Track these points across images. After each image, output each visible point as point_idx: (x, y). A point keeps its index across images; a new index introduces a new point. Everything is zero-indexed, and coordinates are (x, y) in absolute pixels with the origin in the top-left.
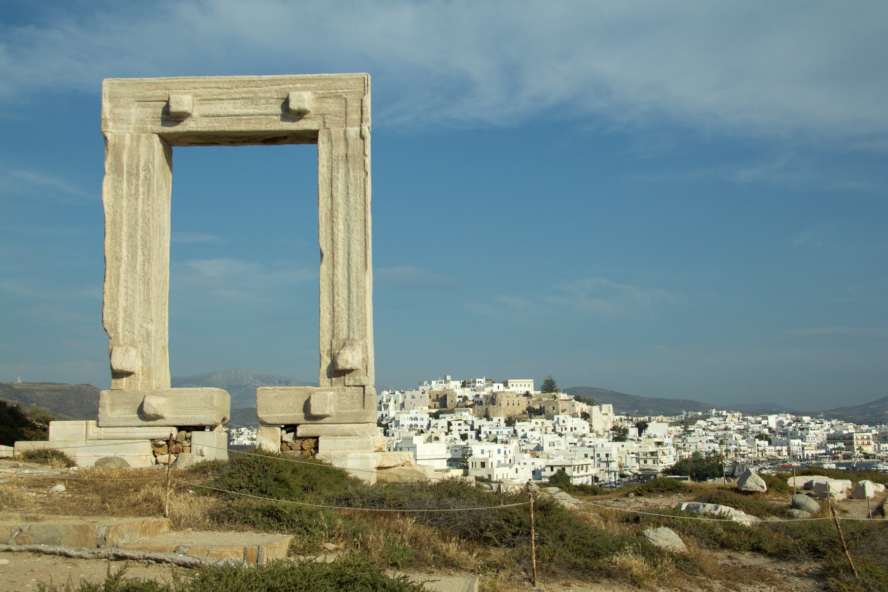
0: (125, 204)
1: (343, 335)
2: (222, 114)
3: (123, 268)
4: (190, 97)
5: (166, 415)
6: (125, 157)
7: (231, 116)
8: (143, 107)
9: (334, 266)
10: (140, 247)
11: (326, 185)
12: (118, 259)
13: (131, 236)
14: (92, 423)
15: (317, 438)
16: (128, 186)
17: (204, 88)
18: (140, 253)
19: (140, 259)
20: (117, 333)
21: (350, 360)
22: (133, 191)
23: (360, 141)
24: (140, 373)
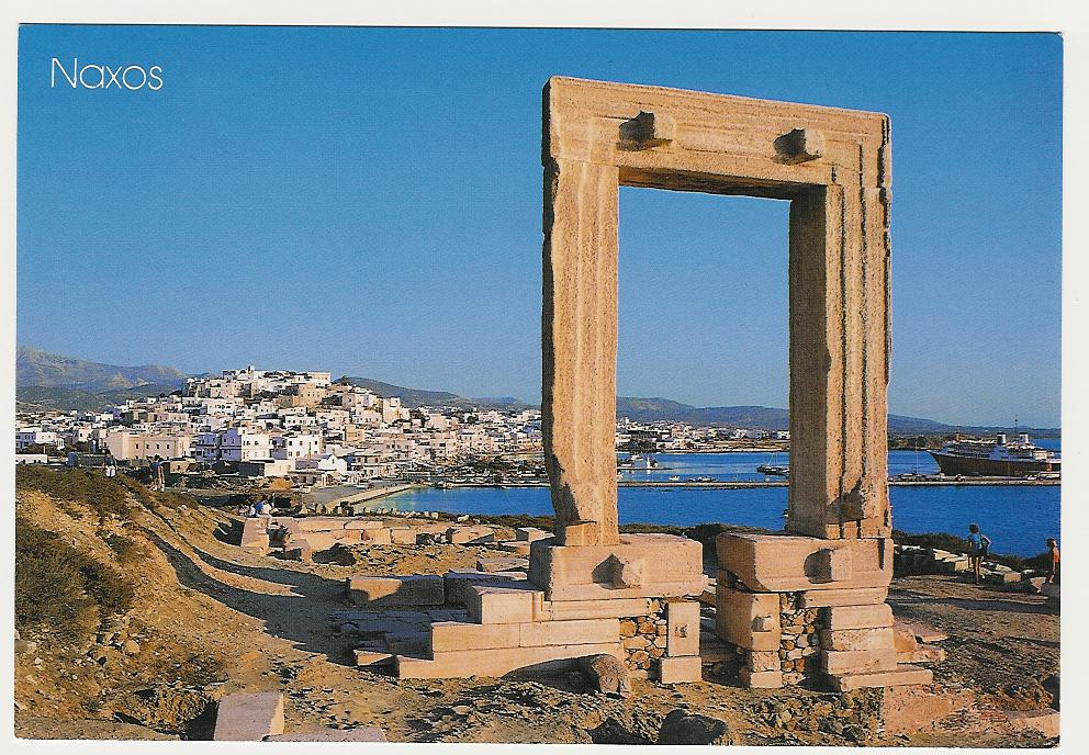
11: (835, 263)
12: (572, 352)
13: (587, 318)
20: (571, 460)
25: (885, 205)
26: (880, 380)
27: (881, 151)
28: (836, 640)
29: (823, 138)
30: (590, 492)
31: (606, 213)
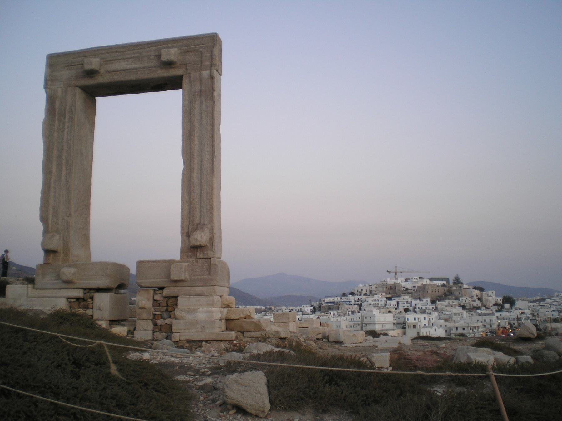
1: (197, 221)
2: (119, 69)
3: (53, 178)
4: (98, 60)
5: (75, 280)
6: (57, 104)
7: (125, 70)
13: (59, 157)
14: (31, 286)
15: (176, 297)
17: (108, 53)
18: (64, 168)
19: (64, 172)
21: (199, 238)
24: (62, 251)
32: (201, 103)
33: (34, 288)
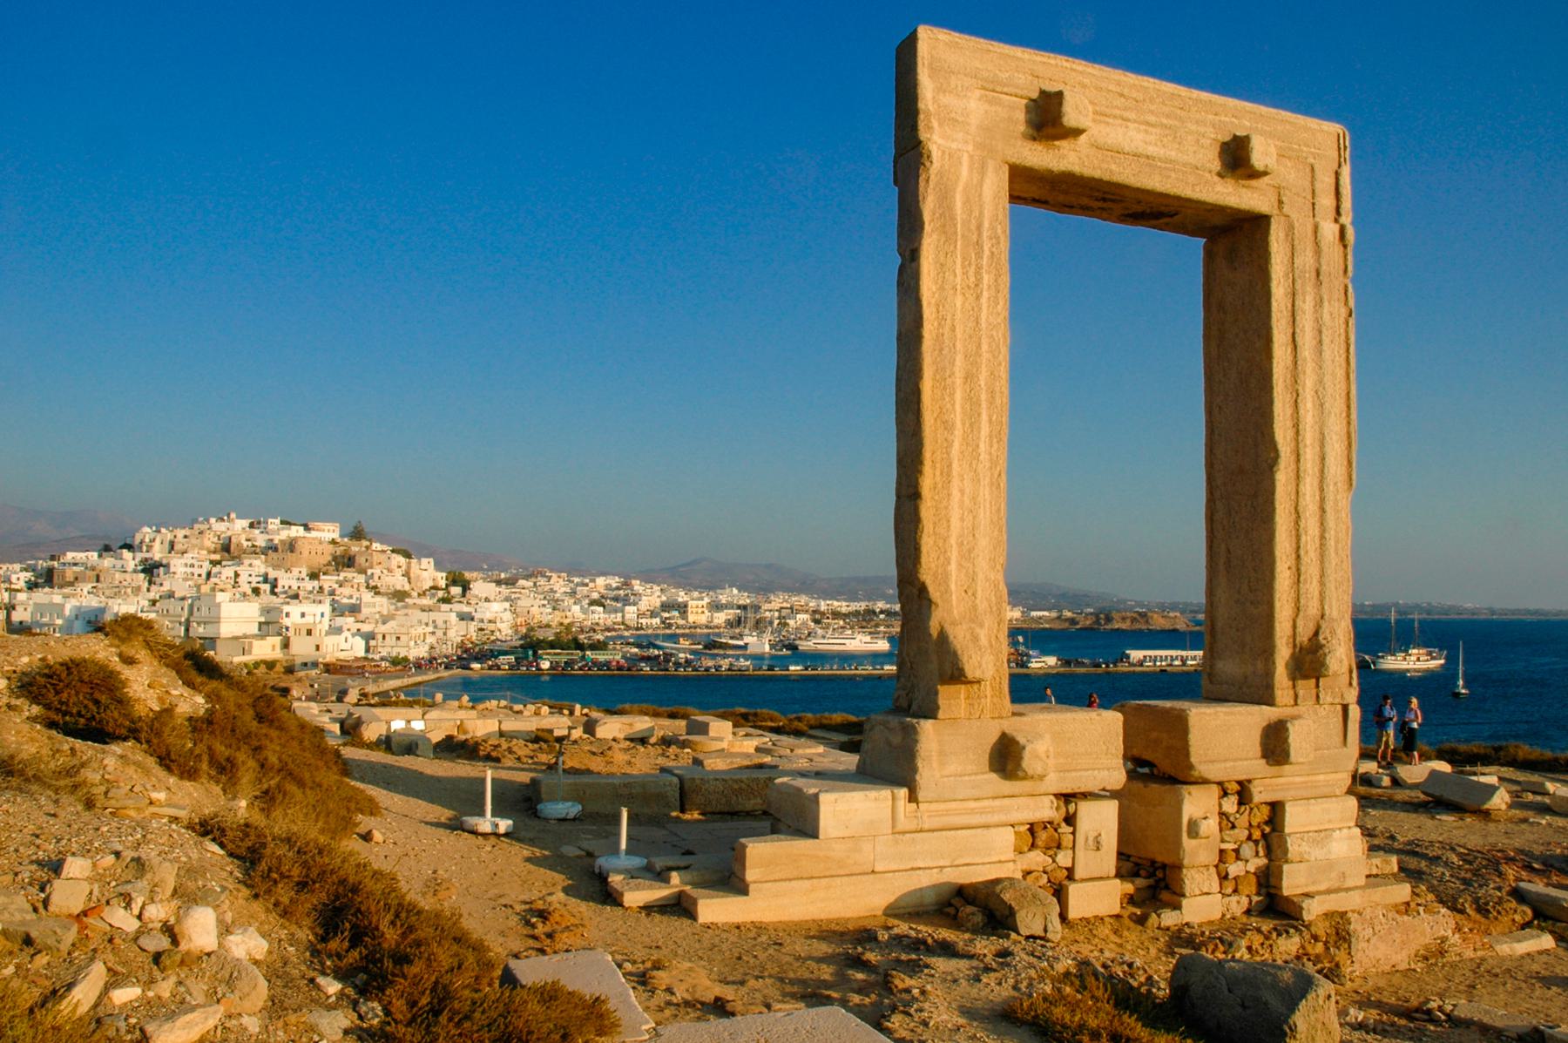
0: (959, 302)
8: (990, 102)
9: (1298, 477)
10: (984, 405)
12: (948, 426)
13: (969, 377)
14: (903, 792)
16: (963, 267)
18: (984, 417)
20: (947, 590)
22: (972, 279)
23: (1338, 249)
25: (1345, 247)
26: (1342, 486)
27: (1337, 174)
28: (1294, 846)
29: (1273, 150)
30: (975, 639)
31: (993, 228)
32: (1319, 303)
33: (913, 798)
